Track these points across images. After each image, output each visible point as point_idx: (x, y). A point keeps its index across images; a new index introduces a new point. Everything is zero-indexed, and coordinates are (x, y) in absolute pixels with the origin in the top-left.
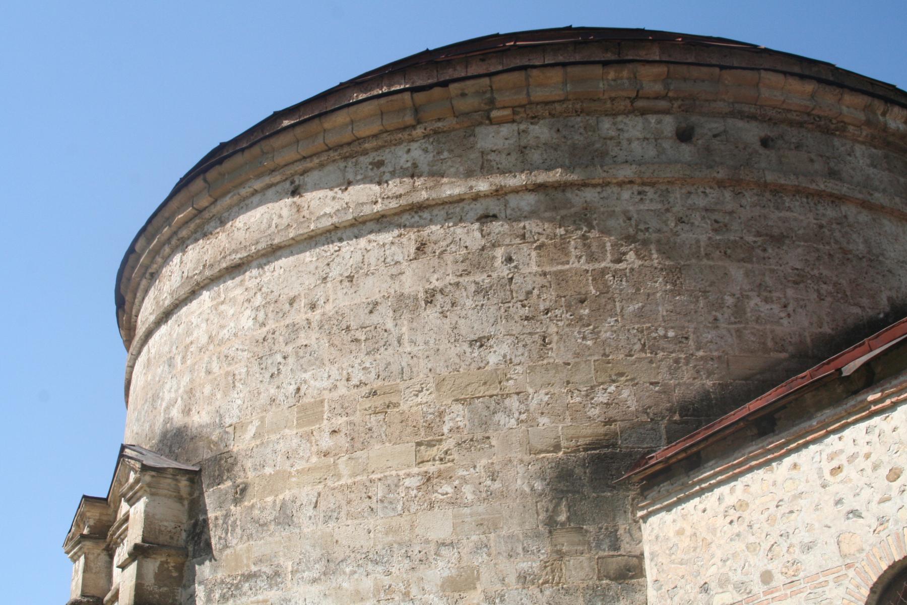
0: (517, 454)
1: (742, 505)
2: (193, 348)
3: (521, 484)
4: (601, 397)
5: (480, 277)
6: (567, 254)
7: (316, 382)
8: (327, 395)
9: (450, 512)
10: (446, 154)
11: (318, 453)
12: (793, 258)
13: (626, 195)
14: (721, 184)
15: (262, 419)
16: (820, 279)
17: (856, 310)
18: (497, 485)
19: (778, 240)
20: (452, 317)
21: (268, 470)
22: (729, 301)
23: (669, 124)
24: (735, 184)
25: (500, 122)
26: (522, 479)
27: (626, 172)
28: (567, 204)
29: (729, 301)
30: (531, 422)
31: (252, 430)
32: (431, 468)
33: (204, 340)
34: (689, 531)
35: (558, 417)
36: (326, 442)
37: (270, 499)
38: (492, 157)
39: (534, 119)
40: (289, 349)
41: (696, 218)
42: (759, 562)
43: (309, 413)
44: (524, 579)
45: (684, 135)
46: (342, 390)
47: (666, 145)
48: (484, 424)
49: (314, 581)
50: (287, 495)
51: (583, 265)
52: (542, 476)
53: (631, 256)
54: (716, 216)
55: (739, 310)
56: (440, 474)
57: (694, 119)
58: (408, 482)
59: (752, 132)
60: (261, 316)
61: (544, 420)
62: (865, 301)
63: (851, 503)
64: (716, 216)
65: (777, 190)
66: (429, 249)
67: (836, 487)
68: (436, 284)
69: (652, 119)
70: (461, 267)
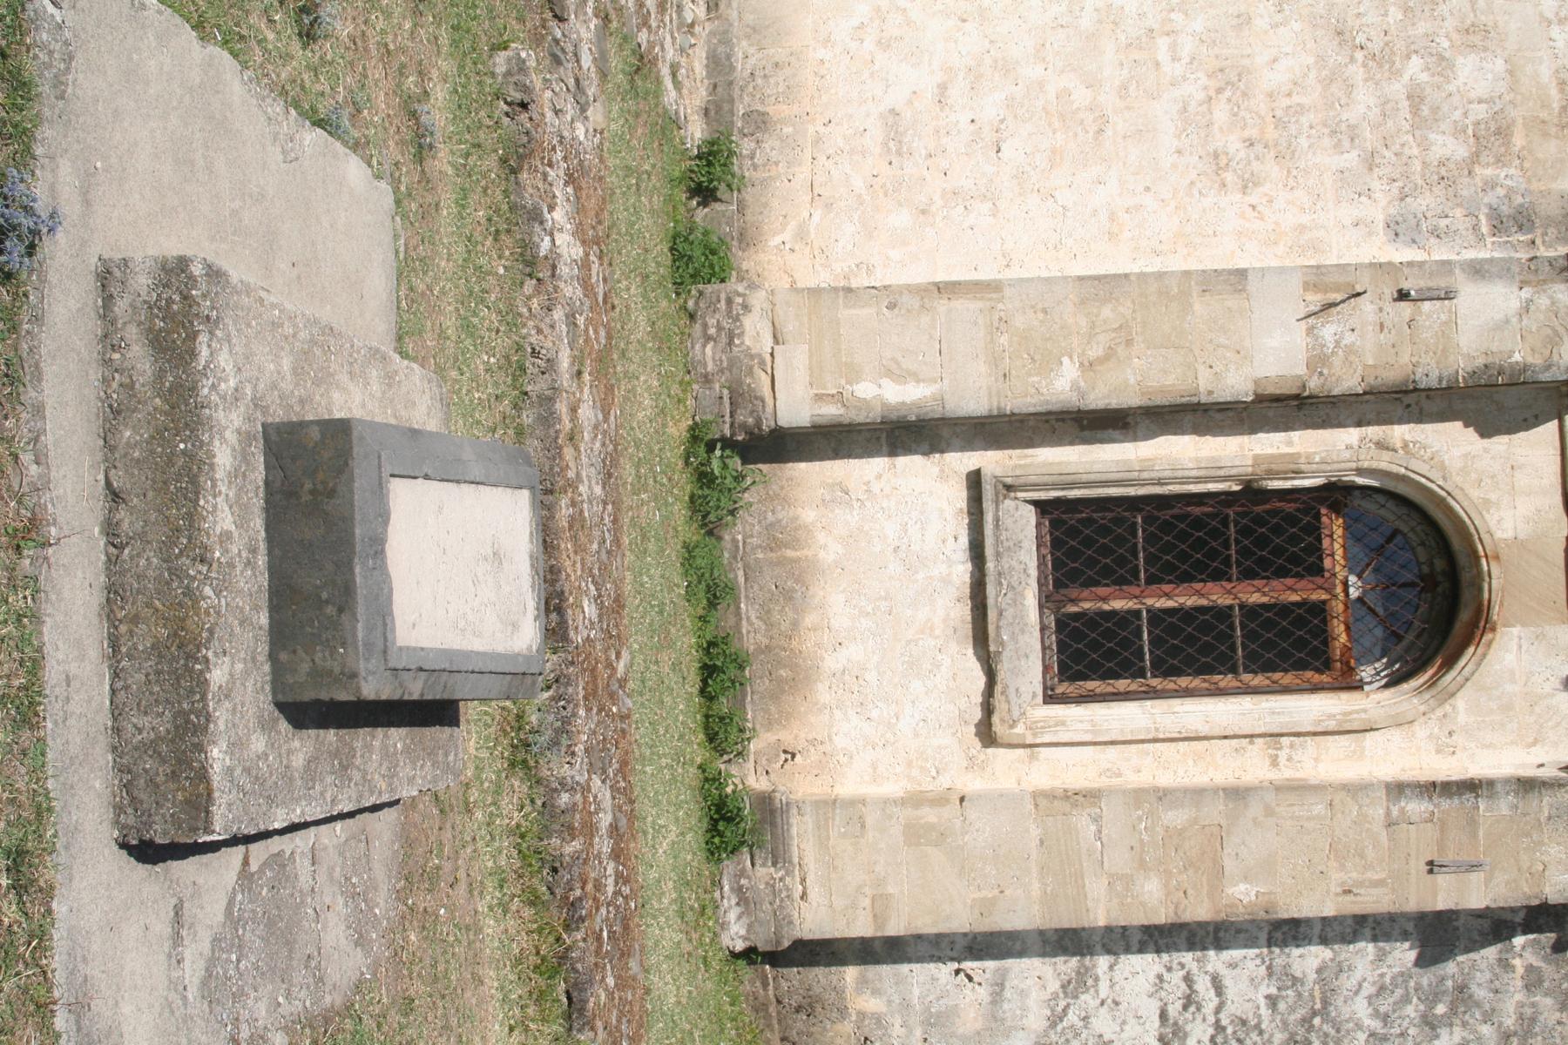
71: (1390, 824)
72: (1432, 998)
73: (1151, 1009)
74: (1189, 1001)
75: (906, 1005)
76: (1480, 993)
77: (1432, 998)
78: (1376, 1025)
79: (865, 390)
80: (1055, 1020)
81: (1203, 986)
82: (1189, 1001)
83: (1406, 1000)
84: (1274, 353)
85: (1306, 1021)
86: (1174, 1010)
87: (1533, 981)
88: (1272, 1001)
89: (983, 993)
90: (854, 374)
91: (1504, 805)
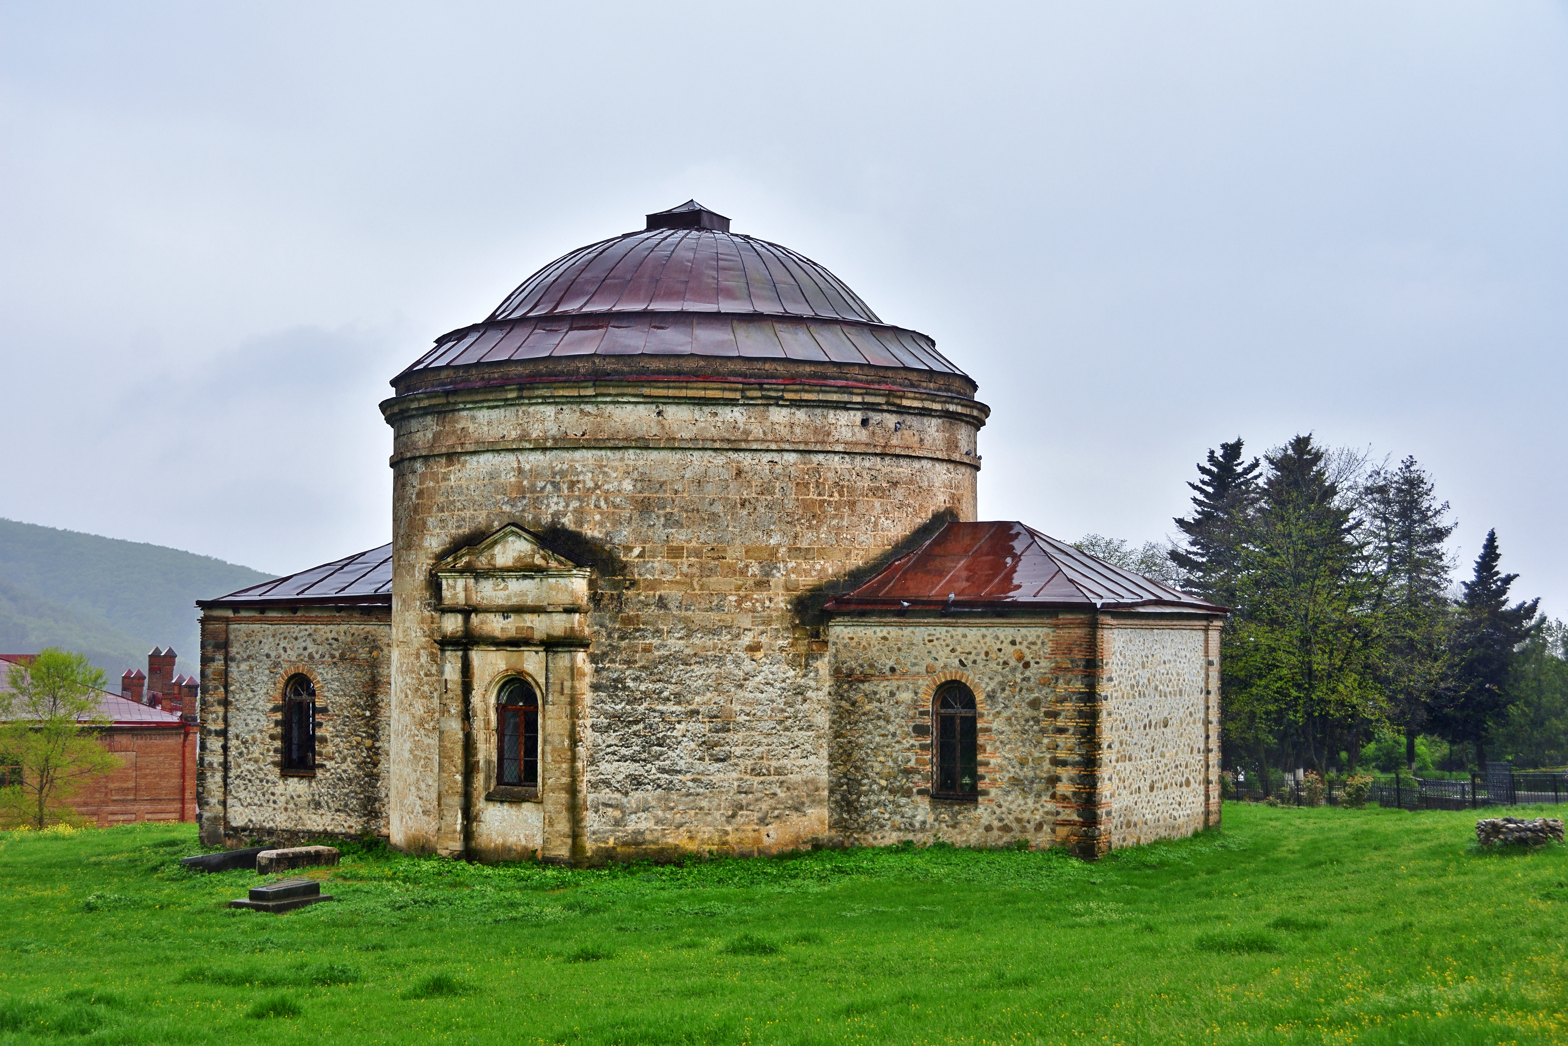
0: (781, 591)
1: (885, 638)
2: (580, 486)
3: (782, 605)
4: (818, 567)
5: (769, 498)
6: (809, 490)
7: (680, 537)
8: (685, 544)
9: (750, 614)
10: (753, 420)
11: (682, 574)
12: (899, 493)
13: (837, 458)
14: (876, 454)
15: (644, 548)
16: (909, 505)
17: (919, 520)
18: (772, 605)
19: (895, 484)
20: (753, 516)
21: (649, 577)
22: (873, 519)
23: (858, 416)
24: (883, 455)
25: (782, 406)
26: (781, 602)
27: (840, 448)
28: (811, 462)
29: (873, 519)
30: (788, 574)
31: (637, 551)
32: (742, 593)
33: (591, 484)
34: (856, 640)
35: (799, 574)
36: (685, 569)
37: (652, 593)
38: (777, 426)
39: (799, 407)
40: (661, 512)
41: (864, 473)
42: (891, 663)
43: (676, 552)
44: (782, 649)
45: (865, 423)
46: (694, 544)
47: (856, 429)
48: (767, 574)
49: (681, 638)
50: (663, 592)
51: (815, 497)
52: (790, 602)
53: (836, 494)
54: (873, 472)
55: (876, 524)
56: (746, 596)
57: (871, 414)
58: (730, 598)
59: (891, 420)
60: (639, 485)
61: (793, 576)
62: (923, 515)
63: (934, 654)
64: (873, 472)
65: (898, 456)
66: (743, 475)
67: (929, 645)
68: (745, 496)
69: (852, 413)
70: (759, 489)
71: (553, 704)
72: (616, 688)
73: (616, 764)
74: (614, 753)
75: (613, 831)
76: (616, 675)
77: (616, 688)
78: (623, 704)
79: (459, 828)
80: (618, 790)
81: (609, 750)
82: (614, 753)
83: (617, 695)
84: (454, 726)
85: (622, 722)
86: (616, 758)
87: (613, 661)
88: (615, 731)
89: (610, 810)
90: (455, 831)
91: (551, 676)
